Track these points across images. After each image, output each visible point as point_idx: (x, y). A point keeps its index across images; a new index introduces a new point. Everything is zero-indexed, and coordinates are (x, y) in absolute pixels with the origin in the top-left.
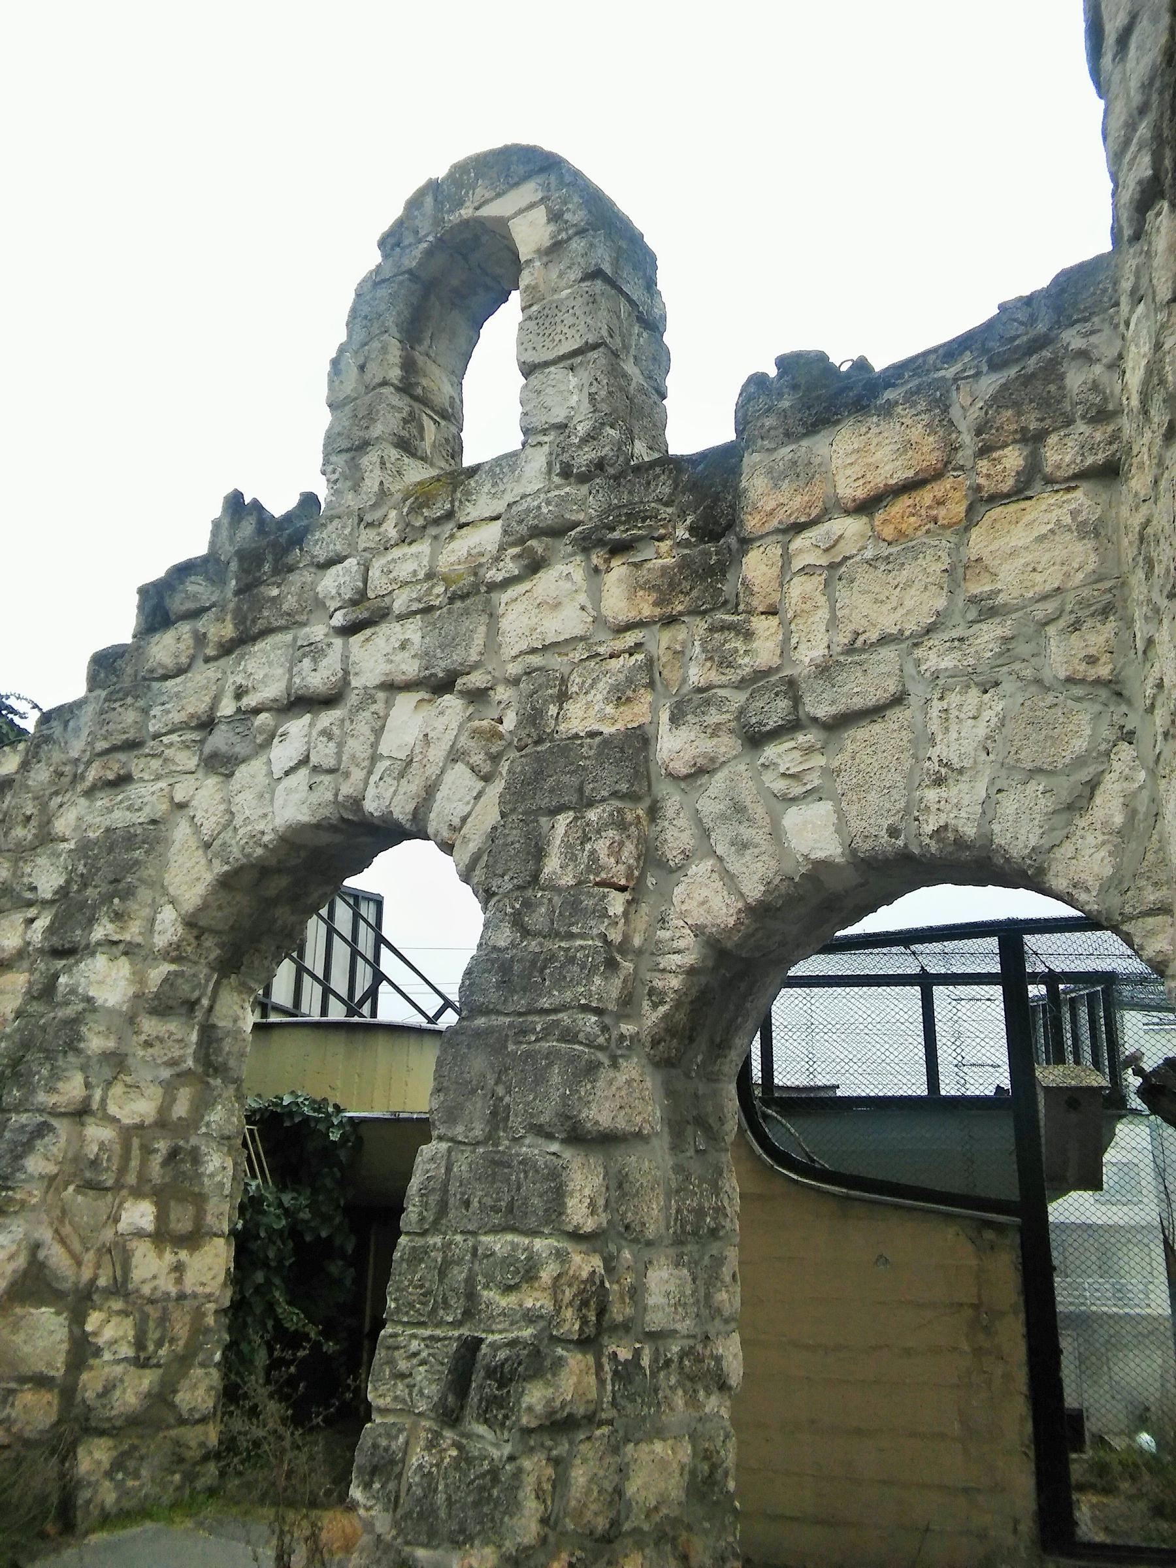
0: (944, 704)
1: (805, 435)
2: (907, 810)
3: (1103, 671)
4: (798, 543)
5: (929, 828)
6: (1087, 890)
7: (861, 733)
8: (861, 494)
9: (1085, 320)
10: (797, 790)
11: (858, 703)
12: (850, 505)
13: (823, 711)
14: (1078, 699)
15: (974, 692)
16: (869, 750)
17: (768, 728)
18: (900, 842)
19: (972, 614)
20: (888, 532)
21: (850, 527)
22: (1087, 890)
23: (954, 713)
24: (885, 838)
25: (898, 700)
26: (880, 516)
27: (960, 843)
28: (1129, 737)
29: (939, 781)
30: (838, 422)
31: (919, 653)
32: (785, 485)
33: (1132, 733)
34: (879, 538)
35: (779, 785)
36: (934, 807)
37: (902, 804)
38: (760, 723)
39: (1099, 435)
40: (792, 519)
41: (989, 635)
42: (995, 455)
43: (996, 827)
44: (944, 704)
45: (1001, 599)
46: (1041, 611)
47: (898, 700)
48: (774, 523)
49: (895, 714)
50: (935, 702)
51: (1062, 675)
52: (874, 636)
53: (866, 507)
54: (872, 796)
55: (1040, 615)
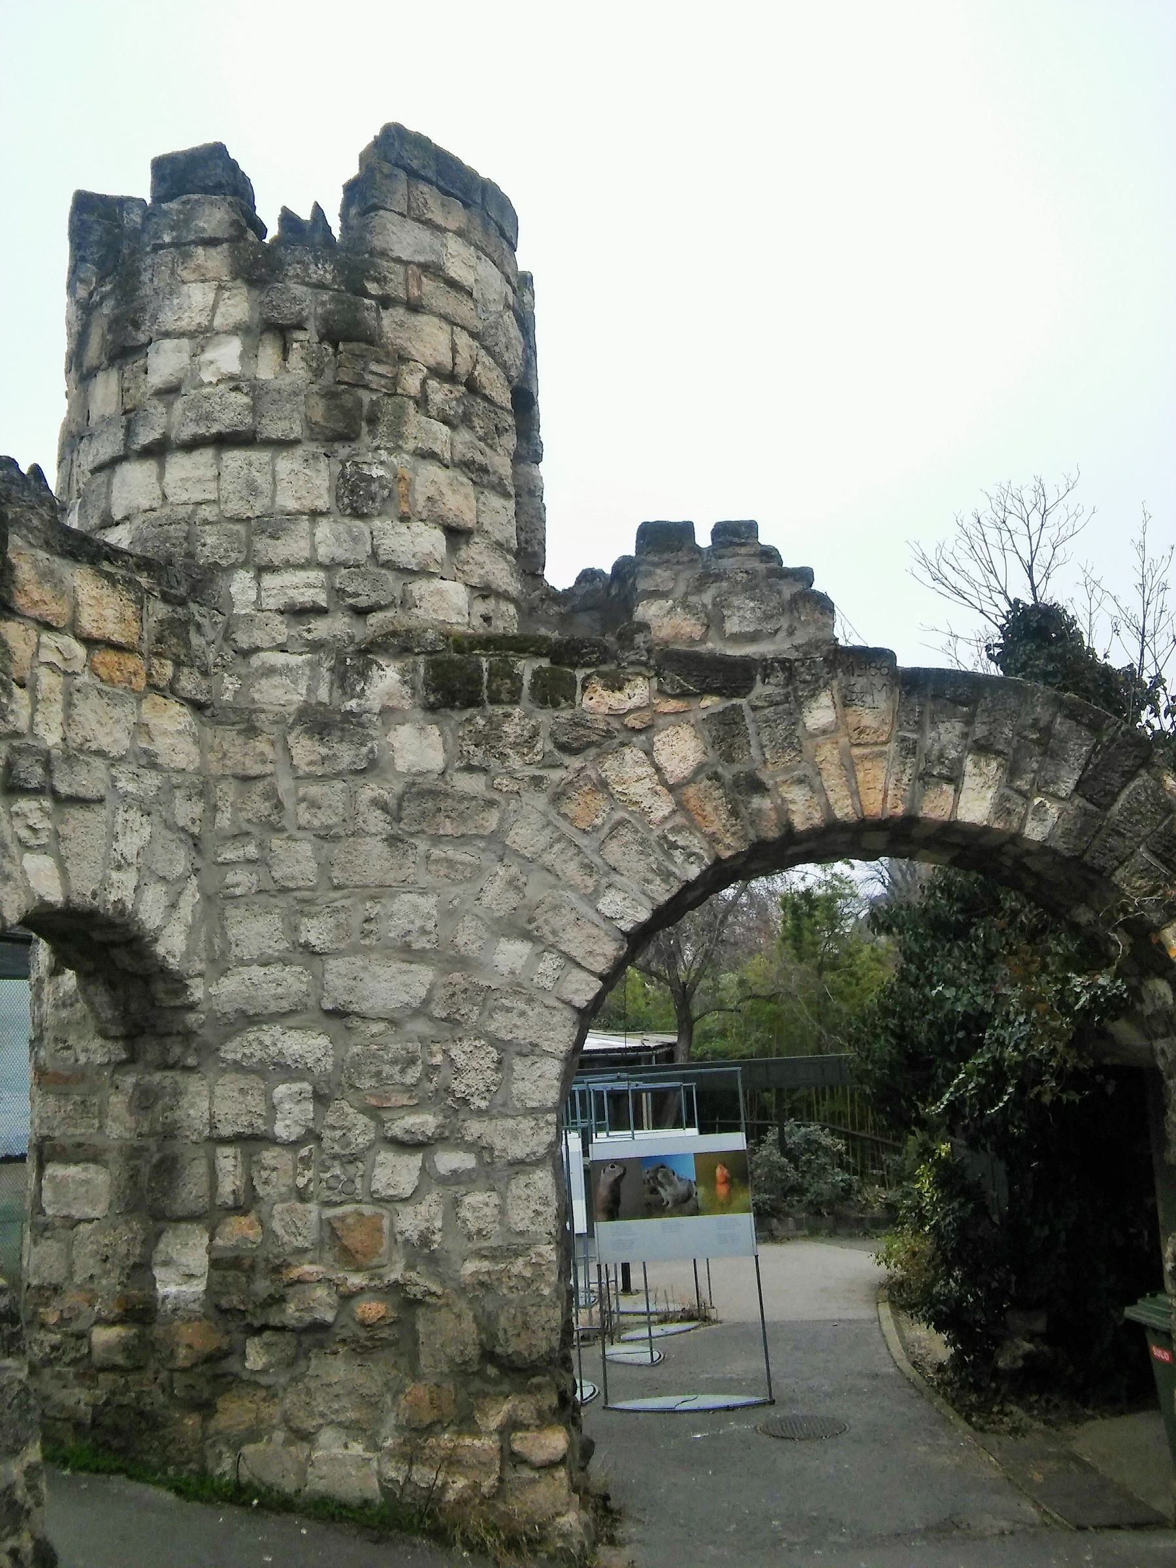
0: (126, 816)
1: (59, 555)
2: (102, 882)
3: (196, 830)
4: (45, 638)
5: (112, 898)
6: (174, 956)
7: (77, 814)
8: (96, 634)
9: (201, 605)
10: (33, 842)
11: (83, 792)
12: (85, 635)
13: (63, 789)
14: (181, 840)
15: (139, 814)
16: (83, 830)
17: (29, 786)
18: (96, 903)
19: (143, 761)
20: (103, 671)
21: (80, 651)
22: (174, 956)
23: (130, 824)
24: (89, 899)
25: (101, 800)
26: (99, 656)
27: (122, 913)
28: (196, 871)
29: (119, 868)
30: (78, 561)
31: (114, 771)
32: (47, 587)
33: (198, 870)
34: (94, 671)
35: (24, 833)
36: (116, 885)
37: (100, 877)
38: (25, 780)
39: (204, 685)
40: (49, 619)
41: (152, 780)
42: (163, 661)
43: (142, 908)
44: (126, 816)
45: (159, 761)
46: (176, 779)
47: (101, 800)
48: (34, 613)
49: (97, 807)
50: (120, 811)
51: (181, 824)
52: (94, 746)
53: (90, 642)
54: (85, 864)
55: (174, 781)
